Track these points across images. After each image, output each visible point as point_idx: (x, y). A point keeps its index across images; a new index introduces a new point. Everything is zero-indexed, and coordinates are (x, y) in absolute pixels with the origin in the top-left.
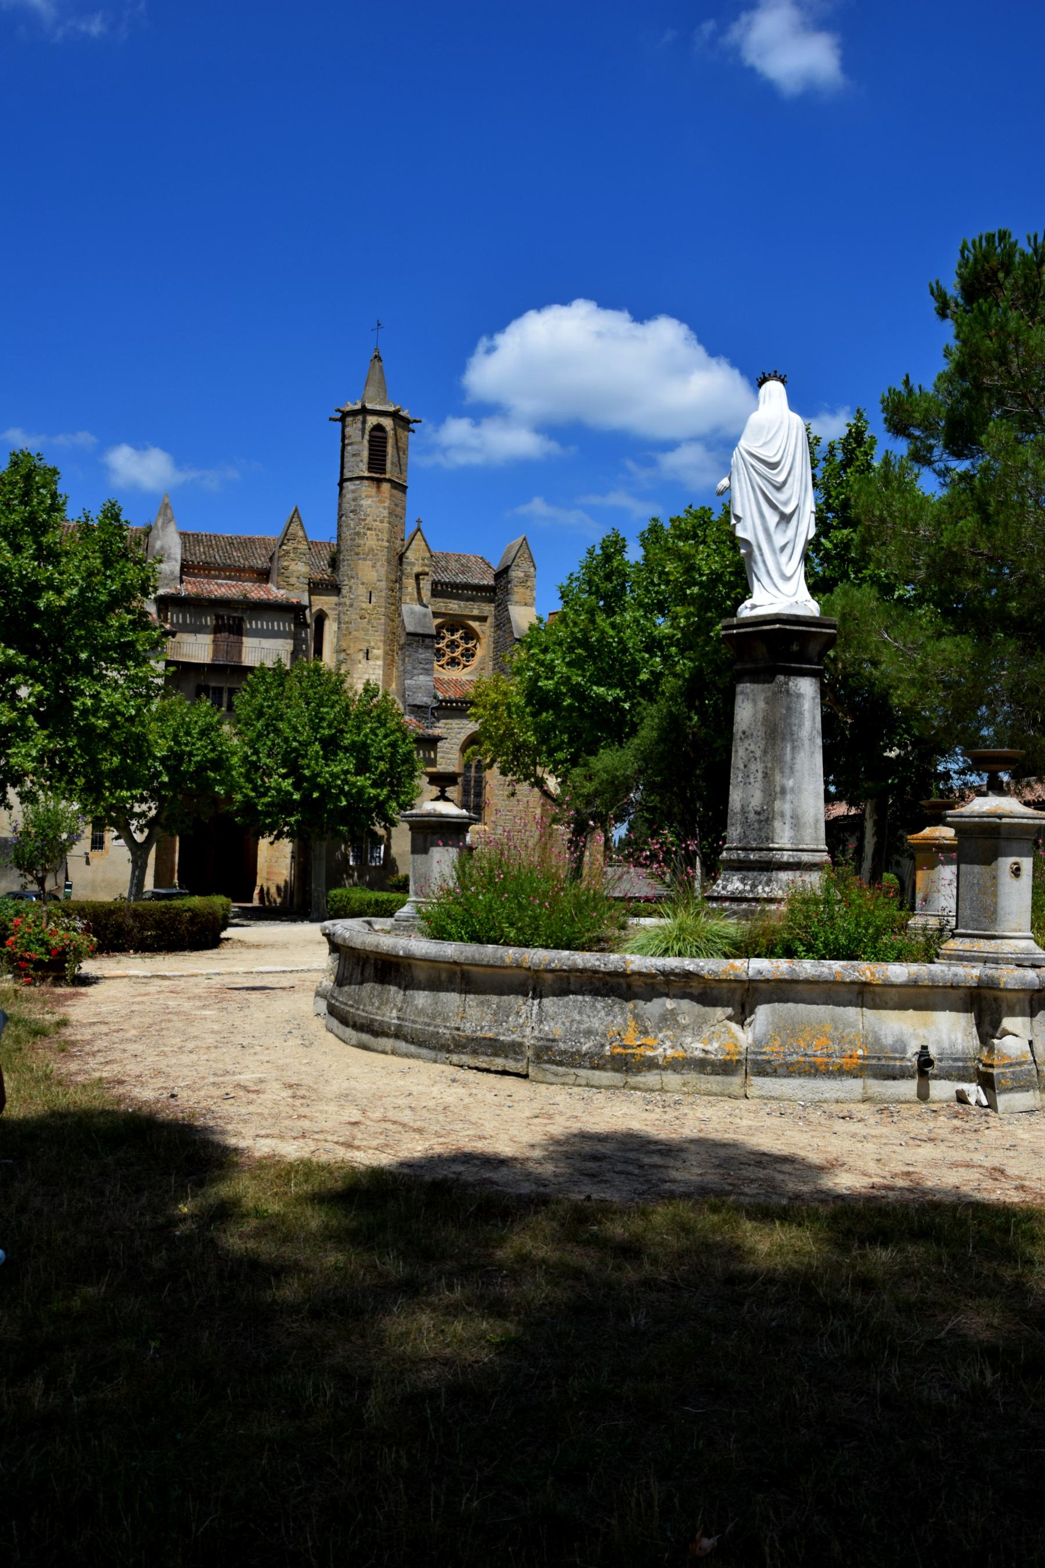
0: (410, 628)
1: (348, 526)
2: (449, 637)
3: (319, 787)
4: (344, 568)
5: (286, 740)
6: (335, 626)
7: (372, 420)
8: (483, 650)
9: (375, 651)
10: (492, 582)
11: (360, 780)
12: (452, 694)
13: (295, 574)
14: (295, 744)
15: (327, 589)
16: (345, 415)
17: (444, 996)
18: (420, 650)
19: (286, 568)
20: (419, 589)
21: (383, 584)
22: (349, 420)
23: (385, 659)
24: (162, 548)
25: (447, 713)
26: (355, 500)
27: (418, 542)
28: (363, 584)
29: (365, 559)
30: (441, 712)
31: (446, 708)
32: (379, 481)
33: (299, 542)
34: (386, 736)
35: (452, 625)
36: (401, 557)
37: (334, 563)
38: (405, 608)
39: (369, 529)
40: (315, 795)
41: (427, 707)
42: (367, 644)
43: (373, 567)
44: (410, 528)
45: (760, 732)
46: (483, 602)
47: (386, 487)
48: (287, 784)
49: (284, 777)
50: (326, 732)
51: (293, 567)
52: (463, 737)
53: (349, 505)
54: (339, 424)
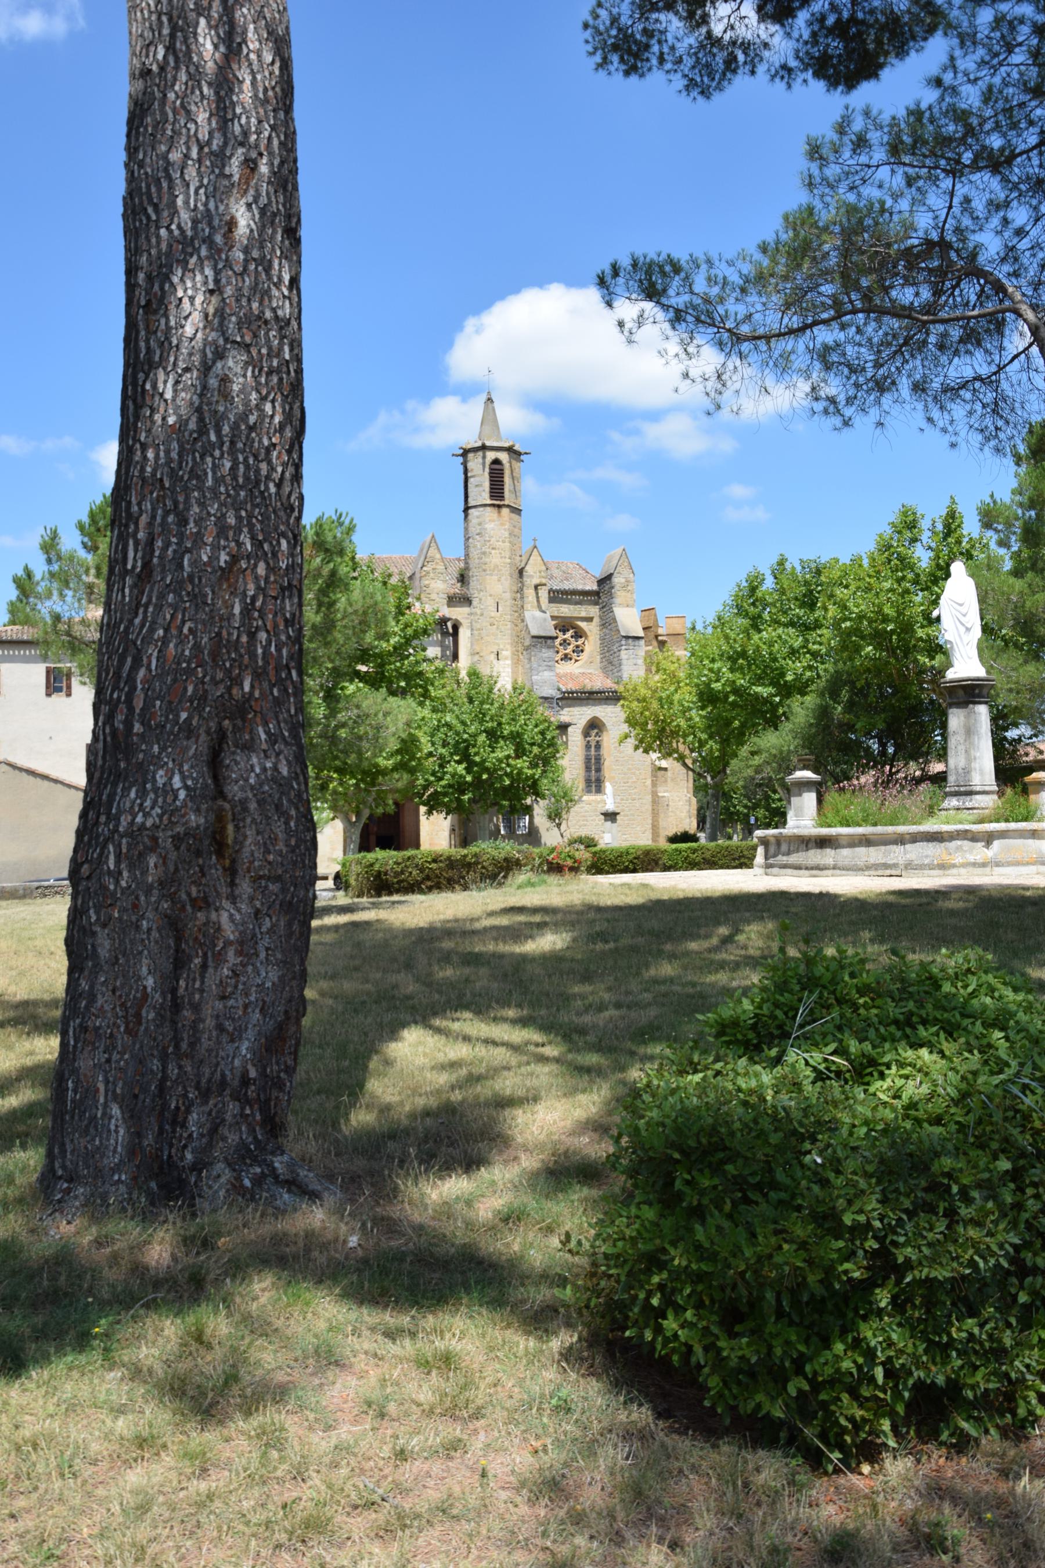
0: (534, 632)
1: (475, 546)
2: (561, 636)
3: (487, 770)
4: (474, 583)
5: (457, 733)
6: (468, 633)
7: (491, 456)
8: (592, 645)
10: (595, 587)
11: (519, 763)
12: (572, 686)
14: (466, 736)
16: (465, 453)
17: (857, 849)
20: (538, 597)
21: (508, 596)
22: (470, 455)
26: (480, 524)
27: (535, 558)
31: (568, 698)
34: (536, 726)
36: (521, 572)
37: (463, 578)
38: (528, 615)
40: (485, 776)
44: (527, 546)
45: (962, 731)
47: (505, 511)
48: (461, 769)
49: (459, 762)
50: (490, 725)
53: (473, 529)
54: (461, 459)
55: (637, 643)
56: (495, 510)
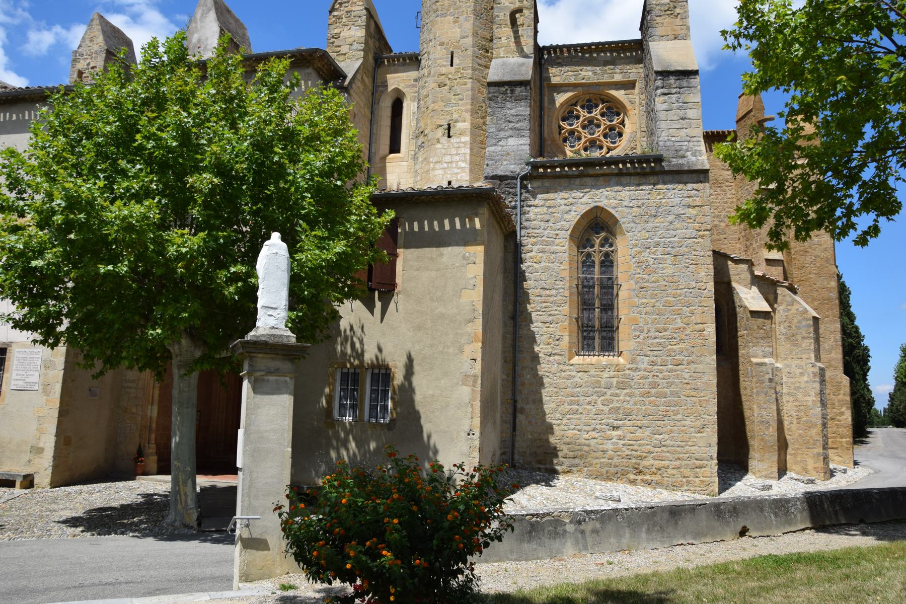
2: (584, 114)
9: (459, 125)
15: (404, 64)
18: (508, 105)
19: (336, 37)
21: (469, 41)
23: (473, 134)
24: (199, 41)
25: (547, 183)
28: (442, 44)
30: (537, 184)
35: (589, 101)
41: (514, 178)
42: (448, 118)
43: (455, 22)
46: (628, 64)
51: (345, 33)
52: (574, 217)
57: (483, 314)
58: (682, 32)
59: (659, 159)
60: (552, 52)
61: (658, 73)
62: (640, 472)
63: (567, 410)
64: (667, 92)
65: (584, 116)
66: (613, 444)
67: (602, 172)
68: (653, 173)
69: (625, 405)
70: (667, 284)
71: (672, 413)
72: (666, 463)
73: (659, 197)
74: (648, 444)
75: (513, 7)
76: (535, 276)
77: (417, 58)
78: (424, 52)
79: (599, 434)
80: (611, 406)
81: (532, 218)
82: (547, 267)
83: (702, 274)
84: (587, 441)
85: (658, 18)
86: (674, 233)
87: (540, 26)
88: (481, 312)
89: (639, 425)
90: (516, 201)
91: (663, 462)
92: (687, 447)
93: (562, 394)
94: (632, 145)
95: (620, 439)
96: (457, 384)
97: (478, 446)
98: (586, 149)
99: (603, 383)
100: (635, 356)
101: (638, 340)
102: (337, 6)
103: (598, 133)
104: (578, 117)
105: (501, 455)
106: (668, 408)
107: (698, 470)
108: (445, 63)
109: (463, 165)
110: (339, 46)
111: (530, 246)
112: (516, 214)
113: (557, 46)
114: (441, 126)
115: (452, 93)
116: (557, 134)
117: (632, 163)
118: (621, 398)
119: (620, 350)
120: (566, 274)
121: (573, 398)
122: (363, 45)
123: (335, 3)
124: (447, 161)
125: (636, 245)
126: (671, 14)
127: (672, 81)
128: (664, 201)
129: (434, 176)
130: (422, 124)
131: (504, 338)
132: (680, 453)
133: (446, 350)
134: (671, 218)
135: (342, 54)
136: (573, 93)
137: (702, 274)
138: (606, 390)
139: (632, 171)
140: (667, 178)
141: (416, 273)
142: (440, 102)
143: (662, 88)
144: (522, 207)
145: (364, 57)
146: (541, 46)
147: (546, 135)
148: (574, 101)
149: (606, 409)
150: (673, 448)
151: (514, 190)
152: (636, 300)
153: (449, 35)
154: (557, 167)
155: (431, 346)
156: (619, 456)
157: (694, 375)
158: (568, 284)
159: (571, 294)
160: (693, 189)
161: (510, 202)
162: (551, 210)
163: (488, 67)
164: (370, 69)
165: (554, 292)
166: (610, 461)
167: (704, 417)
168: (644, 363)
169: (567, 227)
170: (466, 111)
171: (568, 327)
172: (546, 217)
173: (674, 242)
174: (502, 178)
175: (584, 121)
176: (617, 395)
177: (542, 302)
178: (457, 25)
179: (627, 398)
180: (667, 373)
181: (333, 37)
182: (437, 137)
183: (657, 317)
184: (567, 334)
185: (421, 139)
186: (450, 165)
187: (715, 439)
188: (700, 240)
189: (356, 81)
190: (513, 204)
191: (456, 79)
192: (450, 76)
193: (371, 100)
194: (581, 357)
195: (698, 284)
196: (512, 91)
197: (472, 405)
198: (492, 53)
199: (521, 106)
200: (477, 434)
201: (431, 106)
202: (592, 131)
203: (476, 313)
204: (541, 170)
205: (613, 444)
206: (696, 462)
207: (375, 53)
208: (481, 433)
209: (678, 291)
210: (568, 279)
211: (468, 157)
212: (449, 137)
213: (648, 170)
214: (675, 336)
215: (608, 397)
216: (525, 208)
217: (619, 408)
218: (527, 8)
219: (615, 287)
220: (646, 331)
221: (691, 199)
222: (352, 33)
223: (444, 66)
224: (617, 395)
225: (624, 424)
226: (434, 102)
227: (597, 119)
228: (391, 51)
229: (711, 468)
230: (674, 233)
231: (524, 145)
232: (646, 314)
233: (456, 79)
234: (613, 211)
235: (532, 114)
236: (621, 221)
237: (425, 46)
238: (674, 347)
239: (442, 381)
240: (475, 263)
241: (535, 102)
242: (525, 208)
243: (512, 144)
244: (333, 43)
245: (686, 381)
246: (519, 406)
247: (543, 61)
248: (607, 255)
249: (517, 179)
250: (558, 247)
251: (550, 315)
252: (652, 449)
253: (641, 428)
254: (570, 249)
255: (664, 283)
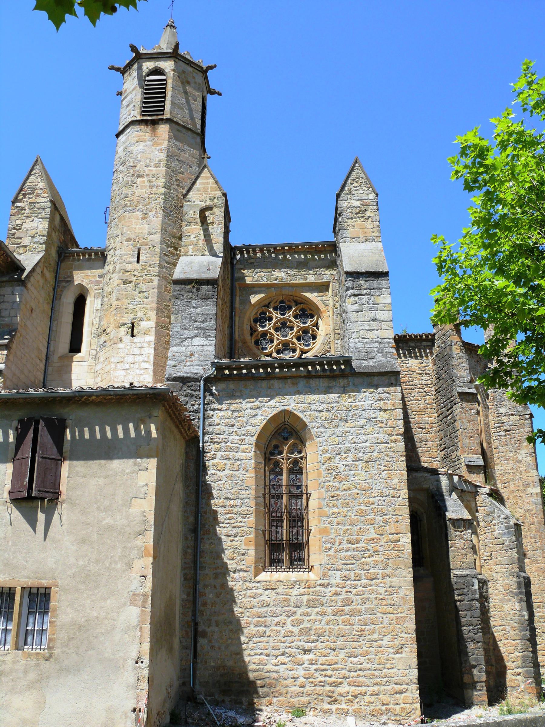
2: (276, 316)
6: (98, 302)
13: (30, 233)
15: (89, 259)
18: (194, 303)
19: (18, 228)
21: (157, 238)
25: (232, 386)
28: (129, 240)
29: (132, 211)
30: (222, 386)
32: (154, 123)
33: (38, 195)
39: (139, 176)
41: (197, 380)
42: (132, 316)
43: (143, 218)
55: (374, 283)
56: (149, 128)
57: (155, 525)
58: (373, 234)
59: (348, 361)
60: (245, 252)
61: (348, 274)
62: (335, 701)
63: (254, 633)
64: (357, 293)
65: (277, 317)
66: (305, 669)
67: (289, 374)
68: (343, 375)
69: (317, 626)
70: (359, 492)
71: (367, 633)
72: (363, 689)
73: (349, 400)
74: (342, 669)
75: (203, 205)
76: (219, 485)
77: (103, 254)
78: (110, 247)
79: (289, 659)
80: (301, 627)
81: (216, 422)
82: (231, 475)
83: (396, 481)
84: (276, 668)
85: (349, 220)
86: (366, 438)
87: (231, 226)
88: (152, 523)
89: (332, 647)
90: (199, 404)
91: (360, 688)
92: (385, 670)
93: (248, 614)
94: (326, 347)
95: (312, 664)
96: (125, 604)
97: (147, 675)
98: (278, 352)
99: (292, 601)
100: (326, 571)
101: (329, 553)
102: (21, 197)
103: (291, 336)
104: (270, 319)
105: (180, 686)
106: (364, 627)
107: (398, 695)
108: (131, 259)
109: (145, 365)
110: (20, 238)
111: (213, 452)
112: (199, 419)
113: (250, 246)
114: (124, 324)
115: (138, 290)
116: (249, 335)
117: (321, 364)
118: (312, 617)
119: (311, 564)
120: (252, 483)
121: (259, 619)
122: (45, 238)
123: (18, 194)
124: (128, 362)
125: (326, 451)
126: (362, 217)
127: (363, 282)
128: (354, 404)
129: (115, 377)
130: (104, 322)
131: (185, 553)
132: (377, 677)
133: (113, 566)
134: (362, 422)
135: (23, 246)
136: (263, 295)
137: (396, 481)
138: (295, 609)
139: (321, 374)
140: (357, 380)
141: (82, 480)
142: (124, 300)
143: (352, 289)
144: (205, 410)
145: (46, 250)
146: (233, 245)
147: (237, 336)
148: (266, 302)
149: (296, 630)
150: (369, 672)
151: (197, 393)
152: (327, 509)
153: (137, 231)
154: (243, 368)
155: (97, 561)
156: (312, 683)
157: (390, 589)
158: (254, 494)
159: (257, 504)
160: (385, 392)
161: (193, 405)
162: (236, 414)
163: (175, 265)
164: (52, 263)
165: (238, 502)
166: (302, 689)
167: (402, 635)
168: (336, 578)
169: (253, 432)
170: (151, 309)
171: (254, 541)
172: (231, 421)
173: (366, 447)
174: (184, 380)
175: (276, 323)
176: (308, 615)
177: (225, 514)
178: (145, 221)
179: (319, 618)
180: (361, 588)
181: (14, 228)
182: (120, 336)
183: (349, 527)
184: (253, 548)
185: (103, 338)
186: (132, 366)
187: (414, 661)
188: (392, 445)
189: (35, 274)
190: (196, 407)
191: (141, 276)
192: (136, 273)
193: (52, 295)
194: (269, 573)
195: (391, 492)
196: (198, 290)
197: (141, 628)
198: (180, 250)
199: (207, 305)
200: (147, 661)
201: (115, 303)
202: (284, 333)
203: (147, 524)
204: (227, 372)
205: (305, 669)
206: (395, 686)
207: (58, 247)
208: (151, 661)
209: (371, 499)
210: (254, 487)
211: (152, 358)
212: (133, 336)
213: (337, 373)
214: (369, 547)
215: (298, 616)
216: (209, 412)
217: (310, 629)
218: (217, 207)
219: (305, 496)
220: (337, 544)
221: (382, 403)
222: (34, 225)
223: (131, 262)
224: (308, 615)
225: (316, 646)
226: (118, 299)
227: (290, 321)
228: (77, 246)
229: (412, 693)
230: (366, 438)
231: (210, 345)
232: (337, 524)
233: (141, 276)
234: (301, 415)
235: (220, 314)
236: (310, 425)
237: (112, 241)
238: (368, 560)
239: (108, 601)
240: (147, 469)
241: (224, 301)
242: (209, 412)
243: (197, 344)
244: (14, 234)
245: (381, 597)
246: (200, 629)
247: (235, 261)
248: (296, 462)
249: (200, 381)
250: (243, 454)
251: (234, 527)
252: (347, 674)
253: (334, 650)
254: (256, 454)
255: (356, 491)
